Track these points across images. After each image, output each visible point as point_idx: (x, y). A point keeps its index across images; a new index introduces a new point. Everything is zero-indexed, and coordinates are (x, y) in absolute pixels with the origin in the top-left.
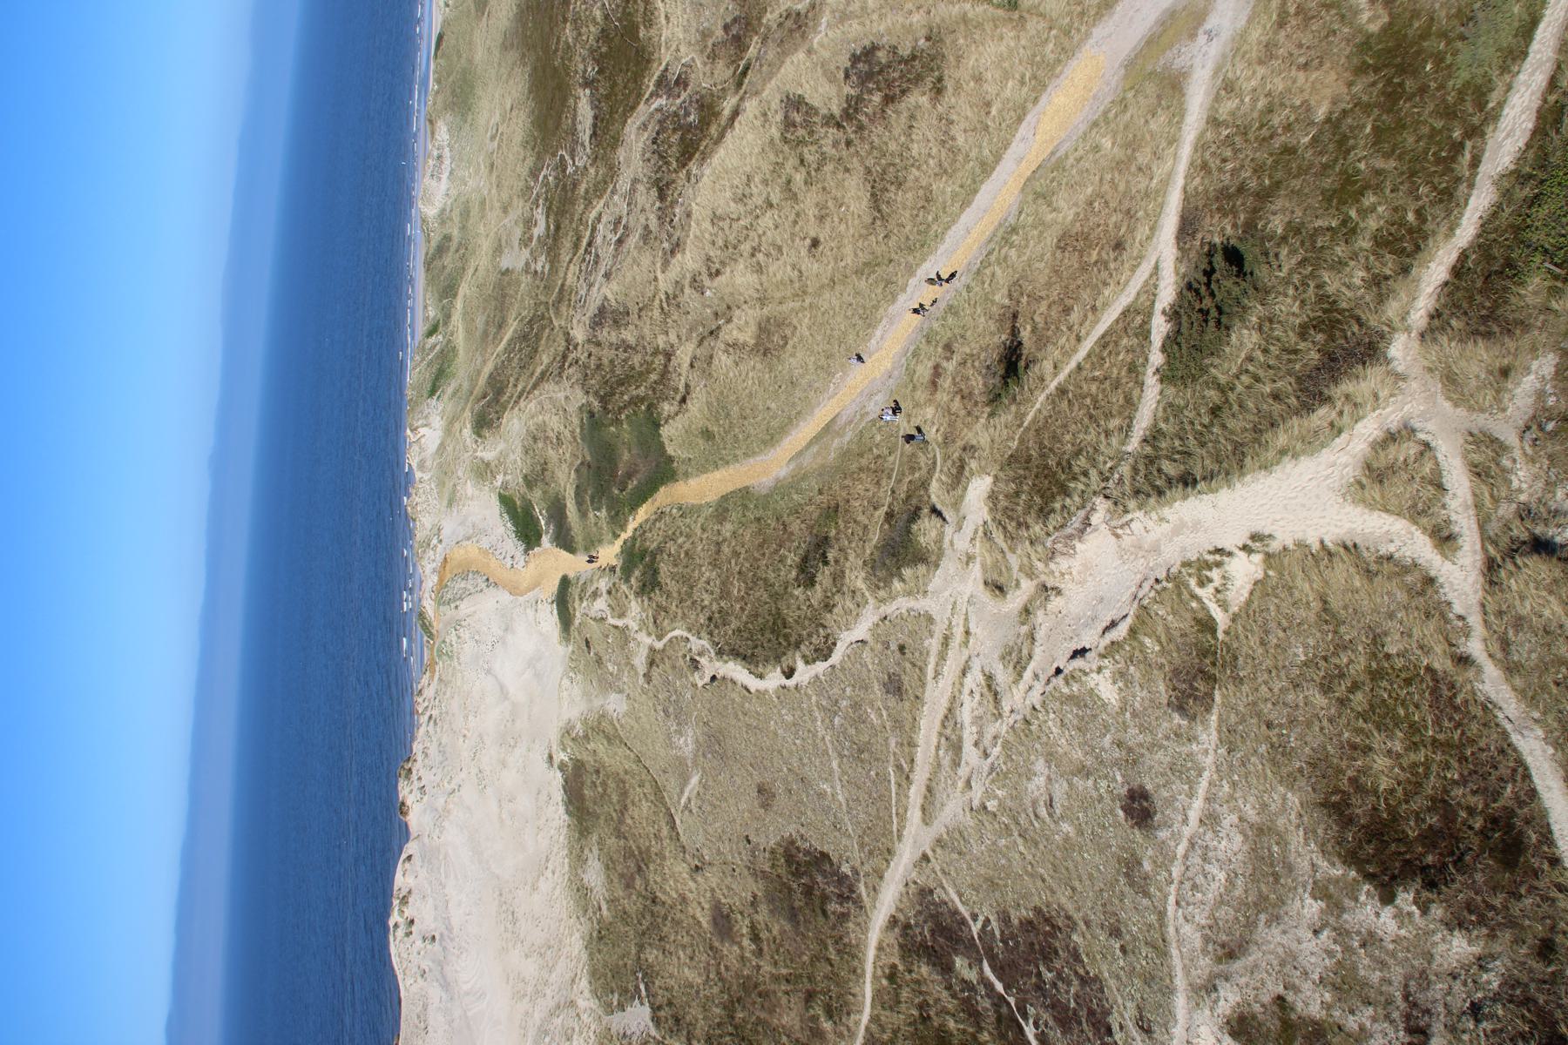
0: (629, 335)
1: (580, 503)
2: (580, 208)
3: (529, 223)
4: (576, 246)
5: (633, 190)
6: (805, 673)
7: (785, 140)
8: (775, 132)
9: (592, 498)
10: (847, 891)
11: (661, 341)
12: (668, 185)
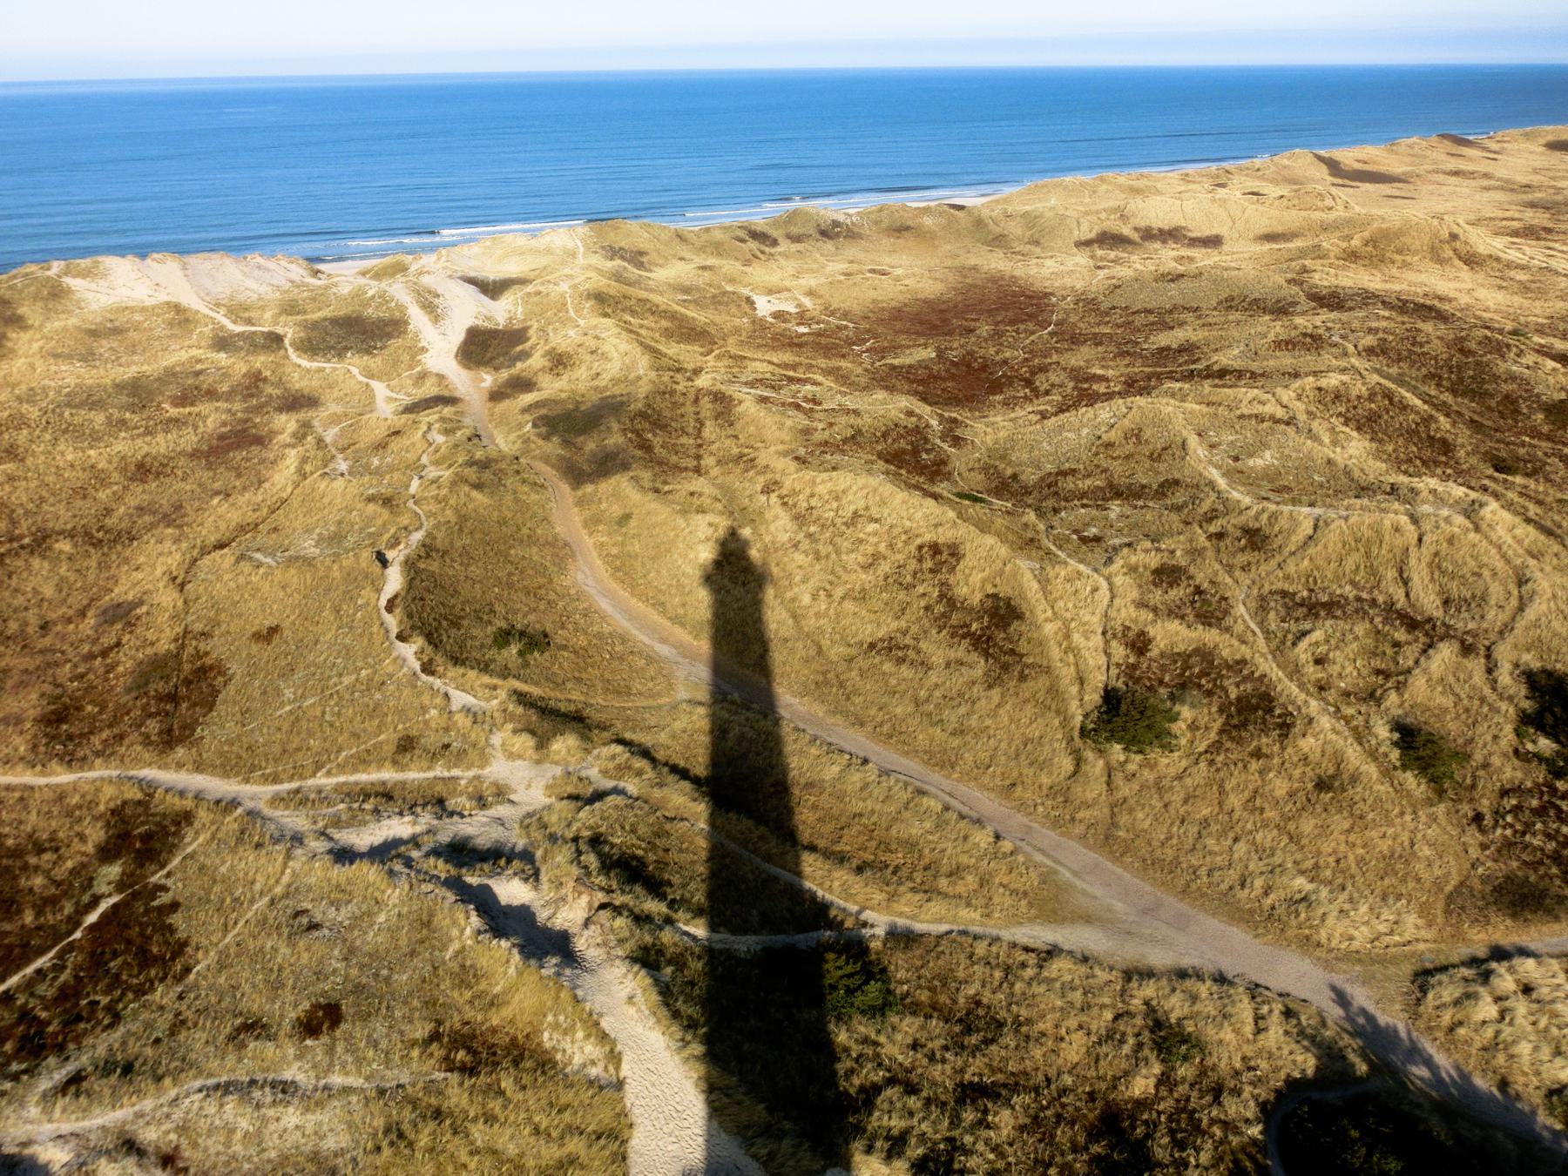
0: (709, 431)
1: (537, 405)
2: (822, 362)
3: (802, 318)
4: (786, 366)
5: (848, 412)
6: (409, 652)
7: (920, 548)
8: (928, 537)
9: (542, 418)
10: (168, 741)
11: (708, 461)
12: (858, 444)
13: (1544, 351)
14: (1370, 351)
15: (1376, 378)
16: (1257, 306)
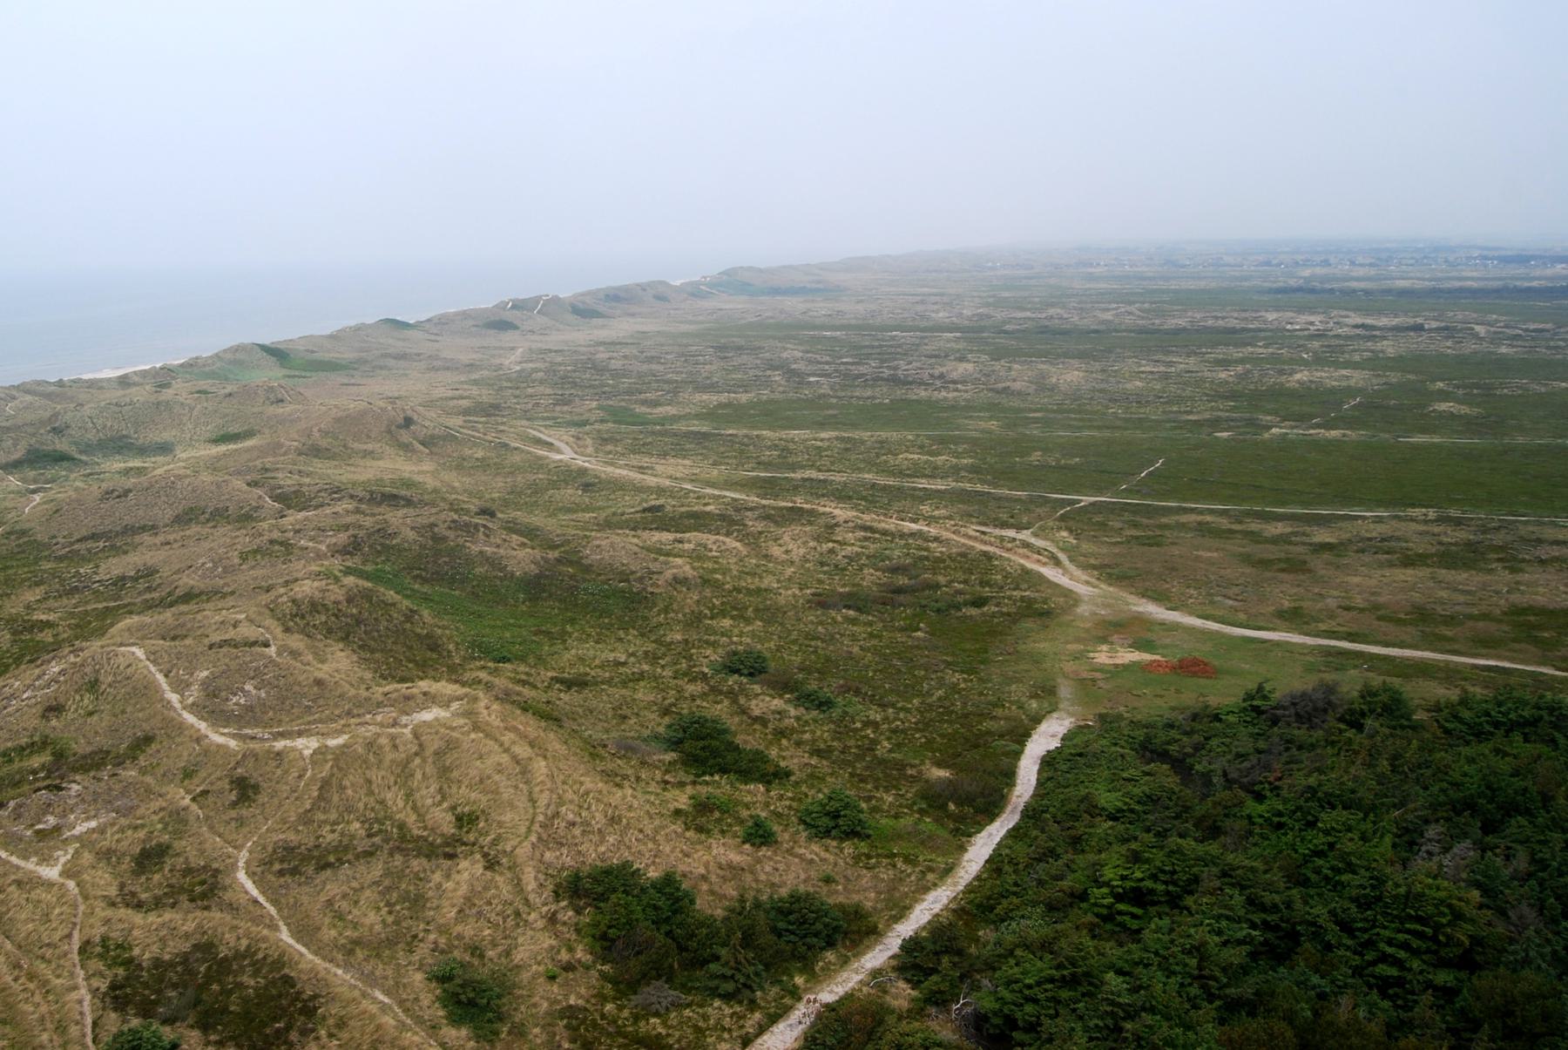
13: (512, 527)
14: (344, 551)
15: (350, 580)
16: (218, 515)
